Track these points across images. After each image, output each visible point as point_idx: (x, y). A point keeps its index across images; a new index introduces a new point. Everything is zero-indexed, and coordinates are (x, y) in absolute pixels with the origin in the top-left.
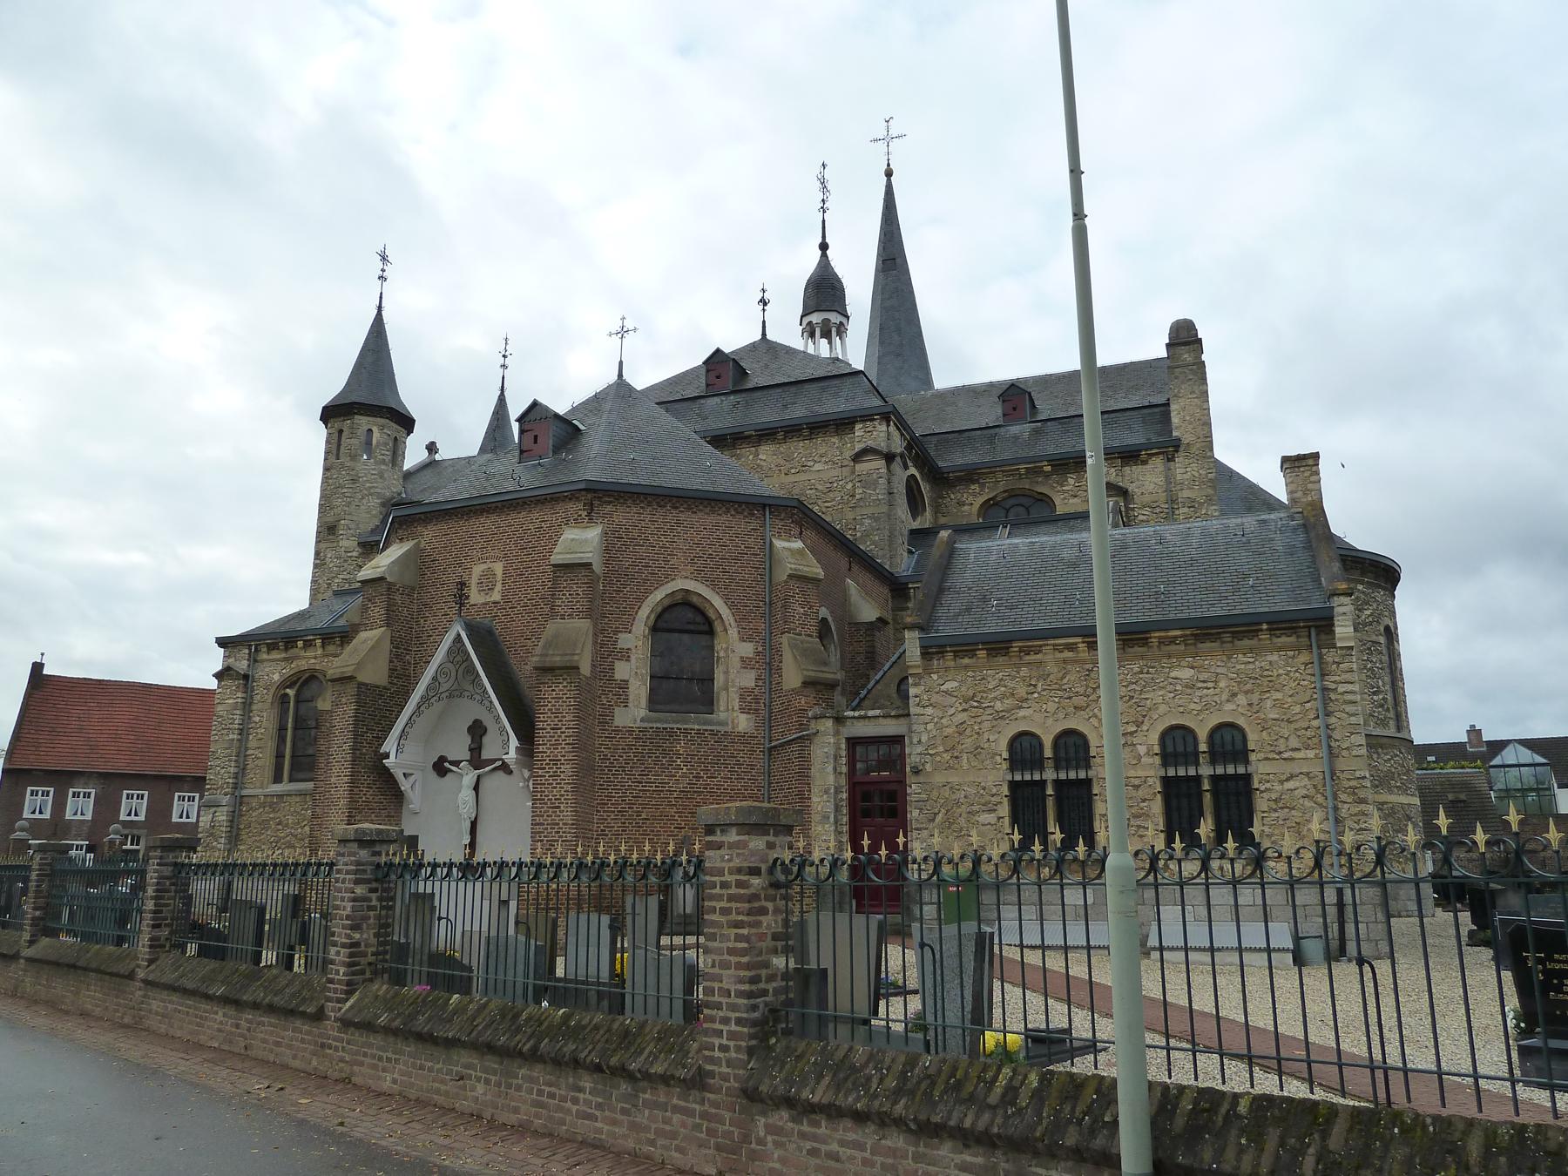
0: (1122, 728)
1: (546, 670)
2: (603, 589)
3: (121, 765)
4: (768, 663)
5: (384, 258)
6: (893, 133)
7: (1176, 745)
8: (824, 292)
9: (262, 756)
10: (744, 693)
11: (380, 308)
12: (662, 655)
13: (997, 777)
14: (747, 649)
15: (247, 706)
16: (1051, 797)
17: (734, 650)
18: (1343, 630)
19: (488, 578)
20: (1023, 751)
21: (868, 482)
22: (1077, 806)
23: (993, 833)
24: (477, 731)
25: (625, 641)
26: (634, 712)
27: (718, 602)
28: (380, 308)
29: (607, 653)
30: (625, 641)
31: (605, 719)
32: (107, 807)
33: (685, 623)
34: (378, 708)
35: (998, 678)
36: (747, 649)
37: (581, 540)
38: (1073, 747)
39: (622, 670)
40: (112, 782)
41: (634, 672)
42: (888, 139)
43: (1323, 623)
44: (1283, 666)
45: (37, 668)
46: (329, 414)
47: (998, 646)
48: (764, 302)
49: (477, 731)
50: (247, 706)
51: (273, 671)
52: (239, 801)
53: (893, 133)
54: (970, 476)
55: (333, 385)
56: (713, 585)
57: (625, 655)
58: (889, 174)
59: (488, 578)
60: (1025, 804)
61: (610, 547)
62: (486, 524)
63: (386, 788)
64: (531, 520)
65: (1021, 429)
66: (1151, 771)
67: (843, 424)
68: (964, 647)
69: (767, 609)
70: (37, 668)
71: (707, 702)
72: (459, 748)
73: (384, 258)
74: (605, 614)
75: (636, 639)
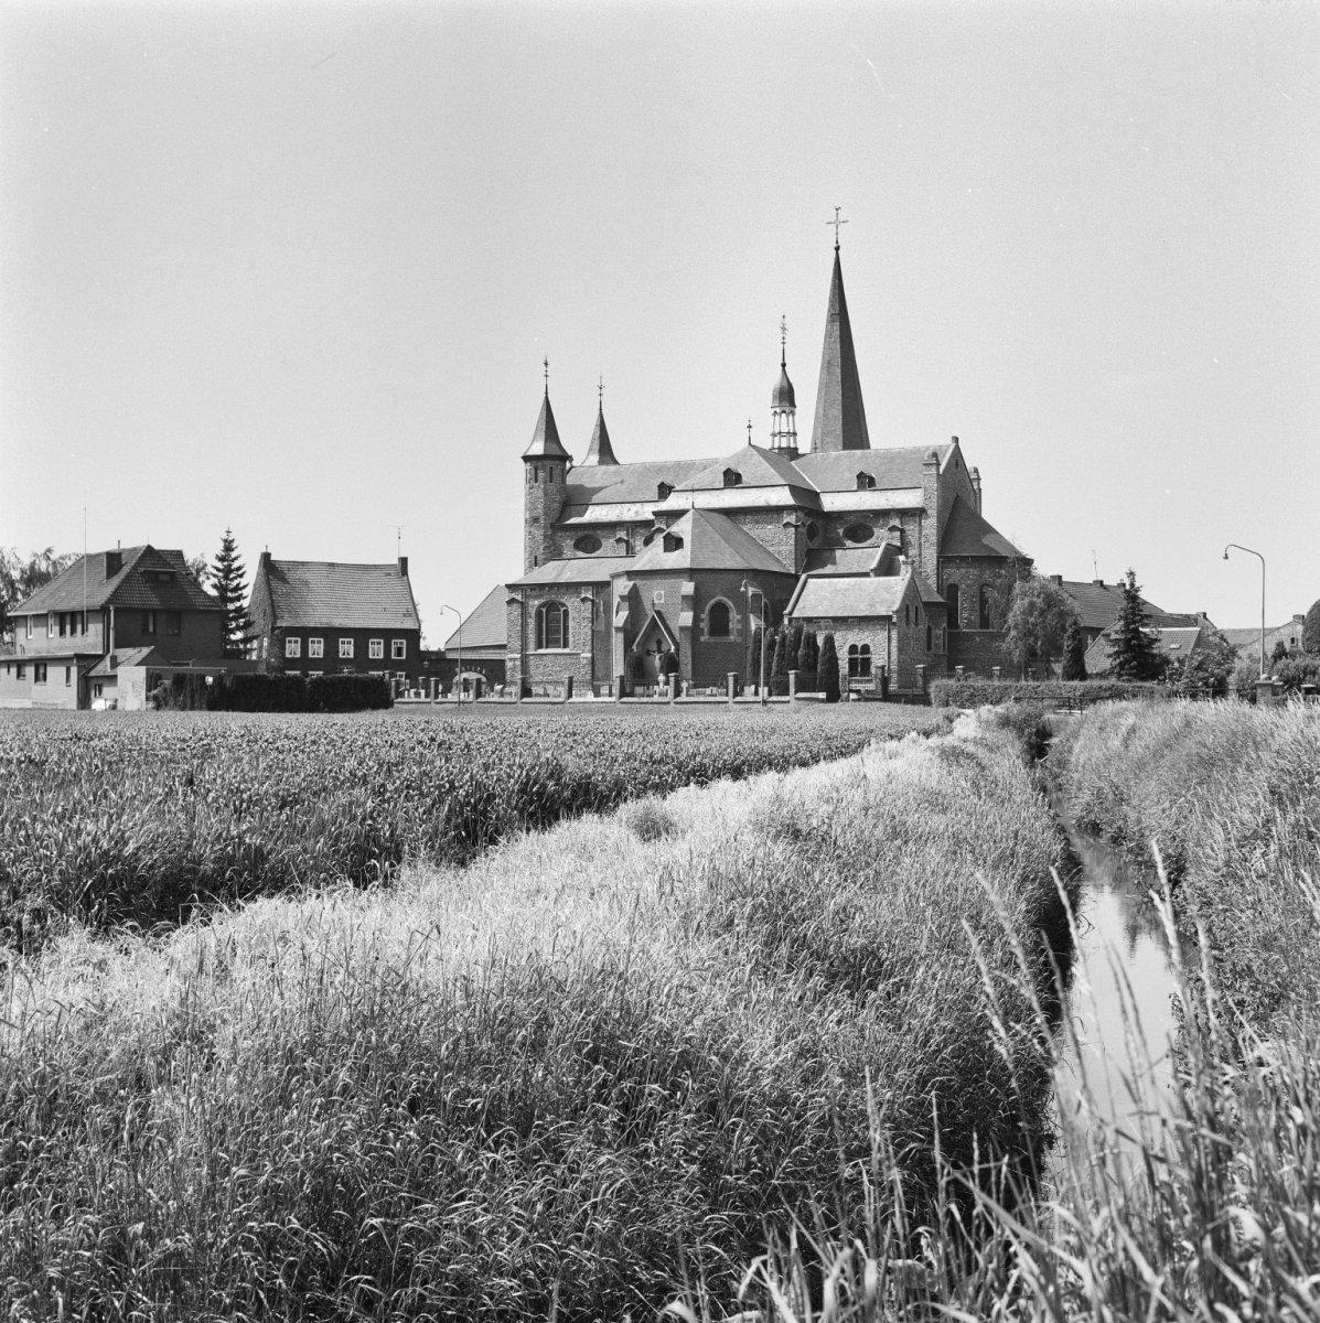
5: (546, 364)
6: (841, 218)
7: (853, 649)
8: (786, 396)
9: (532, 637)
10: (738, 630)
11: (547, 398)
14: (739, 617)
17: (734, 616)
25: (703, 616)
27: (730, 604)
28: (547, 398)
30: (703, 616)
31: (698, 639)
36: (739, 617)
39: (702, 625)
41: (704, 625)
42: (837, 223)
48: (750, 427)
49: (659, 643)
53: (841, 218)
56: (728, 597)
57: (702, 620)
58: (837, 249)
61: (696, 588)
71: (726, 632)
73: (546, 364)
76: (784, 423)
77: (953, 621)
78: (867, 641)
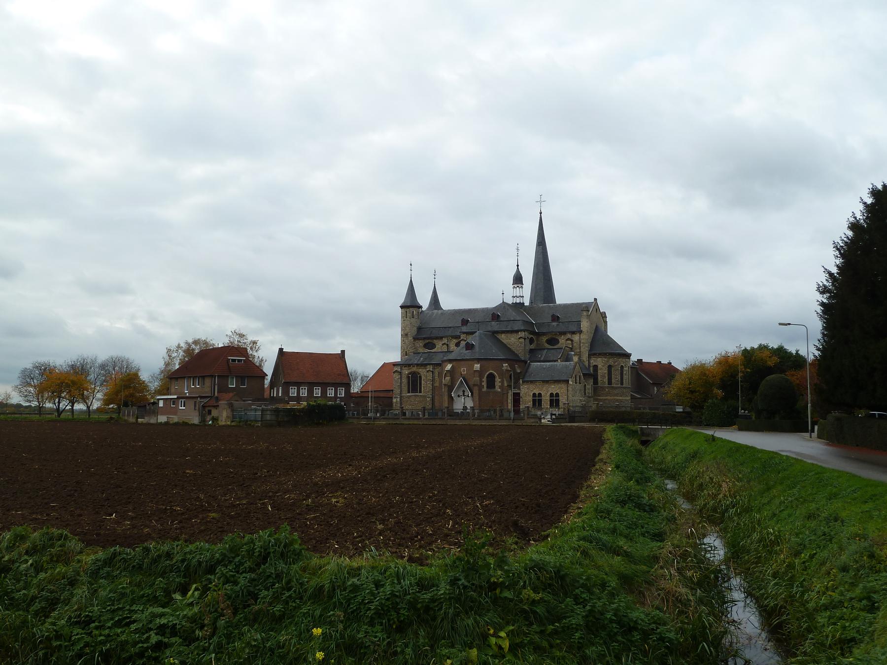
0: (546, 392)
1: (474, 385)
2: (480, 373)
3: (312, 380)
4: (502, 382)
8: (518, 279)
9: (405, 388)
12: (465, 322)
13: (531, 398)
15: (401, 378)
16: (537, 401)
17: (498, 380)
18: (570, 382)
19: (464, 370)
20: (534, 395)
21: (521, 343)
22: (540, 401)
23: (530, 404)
24: (464, 391)
26: (485, 389)
29: (481, 381)
32: (324, 392)
33: (491, 378)
34: (450, 388)
35: (532, 386)
37: (477, 366)
38: (540, 395)
40: (311, 385)
41: (484, 384)
42: (541, 202)
43: (568, 381)
44: (563, 386)
45: (281, 350)
46: (402, 307)
47: (532, 382)
49: (464, 391)
50: (401, 378)
51: (406, 372)
52: (401, 397)
54: (544, 334)
55: (401, 301)
59: (464, 370)
60: (534, 401)
62: (463, 362)
63: (451, 399)
64: (470, 362)
65: (555, 324)
66: (548, 398)
67: (517, 332)
68: (527, 382)
69: (501, 375)
70: (281, 350)
72: (461, 394)
74: (481, 377)
75: (485, 379)
76: (518, 292)
77: (596, 382)
78: (558, 391)
